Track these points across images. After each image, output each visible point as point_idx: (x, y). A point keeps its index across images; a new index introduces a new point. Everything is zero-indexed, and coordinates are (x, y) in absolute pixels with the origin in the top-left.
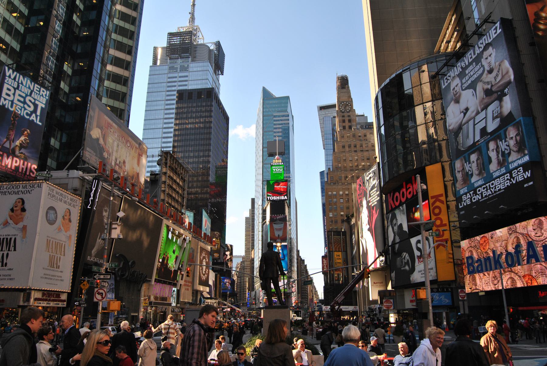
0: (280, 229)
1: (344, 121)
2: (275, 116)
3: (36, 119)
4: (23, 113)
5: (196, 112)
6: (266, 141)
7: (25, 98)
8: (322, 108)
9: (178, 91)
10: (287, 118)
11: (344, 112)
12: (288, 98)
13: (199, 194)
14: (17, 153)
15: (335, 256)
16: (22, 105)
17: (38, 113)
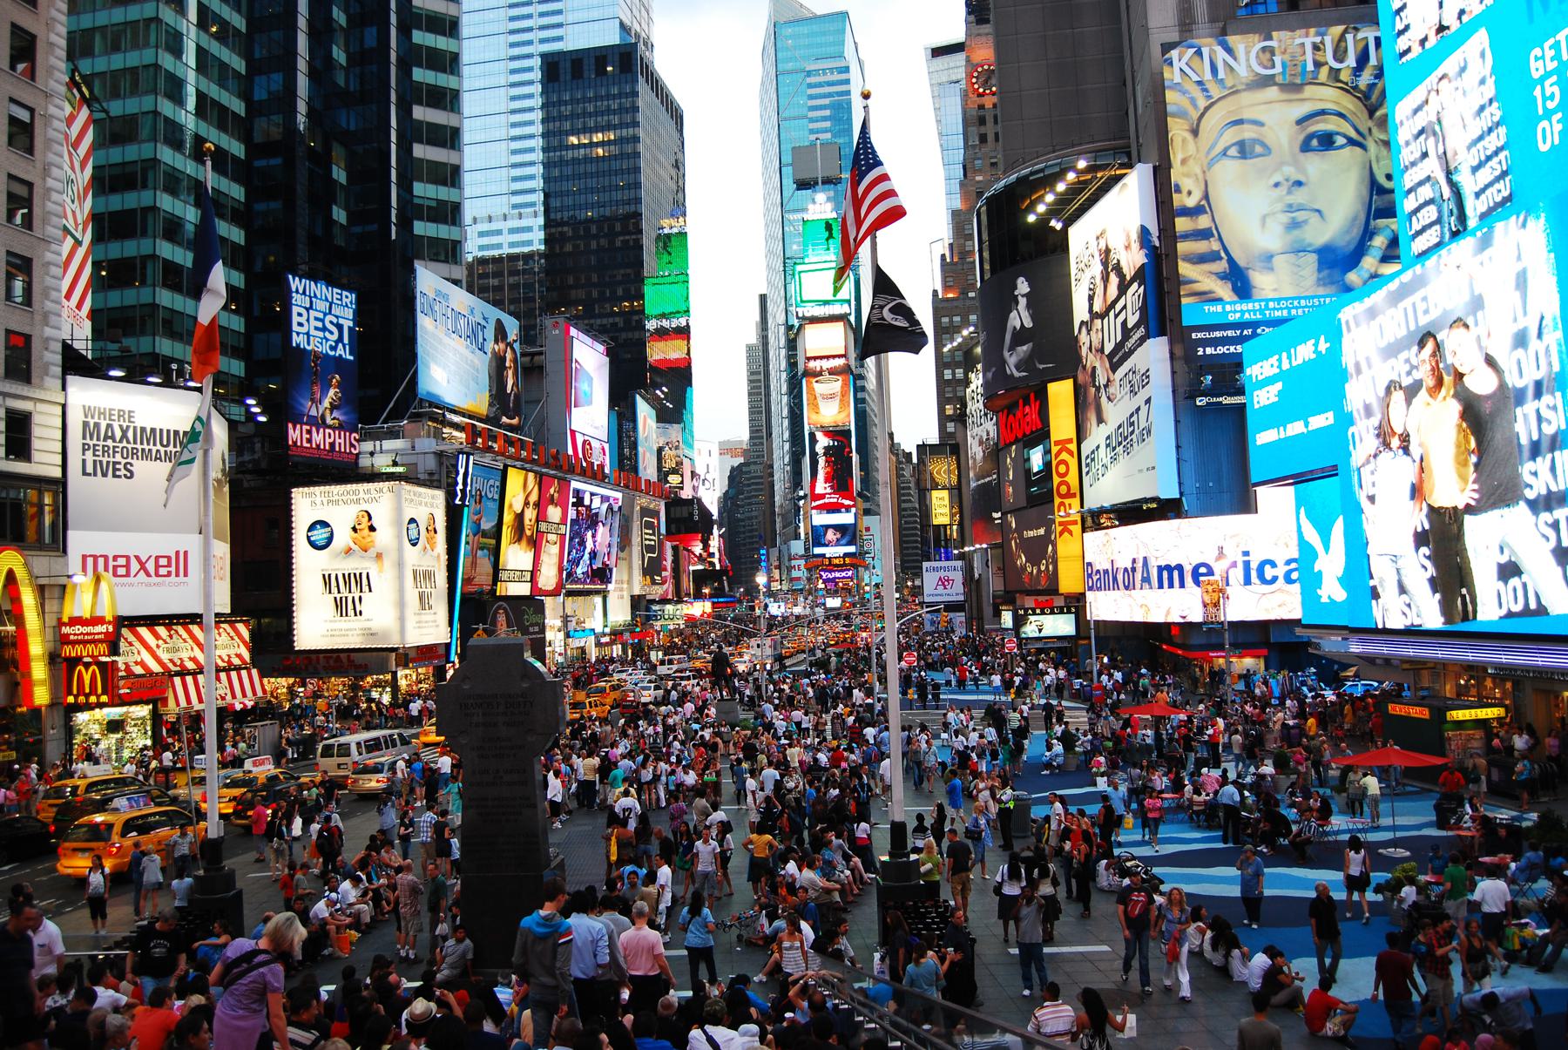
0: (832, 397)
1: (982, 121)
2: (809, 74)
3: (344, 352)
4: (324, 349)
5: (596, 114)
6: (787, 147)
7: (322, 321)
8: (938, 52)
9: (544, 56)
10: (843, 76)
11: (982, 95)
12: (843, 16)
13: (622, 330)
14: (329, 421)
15: (934, 501)
16: (321, 334)
17: (346, 341)
